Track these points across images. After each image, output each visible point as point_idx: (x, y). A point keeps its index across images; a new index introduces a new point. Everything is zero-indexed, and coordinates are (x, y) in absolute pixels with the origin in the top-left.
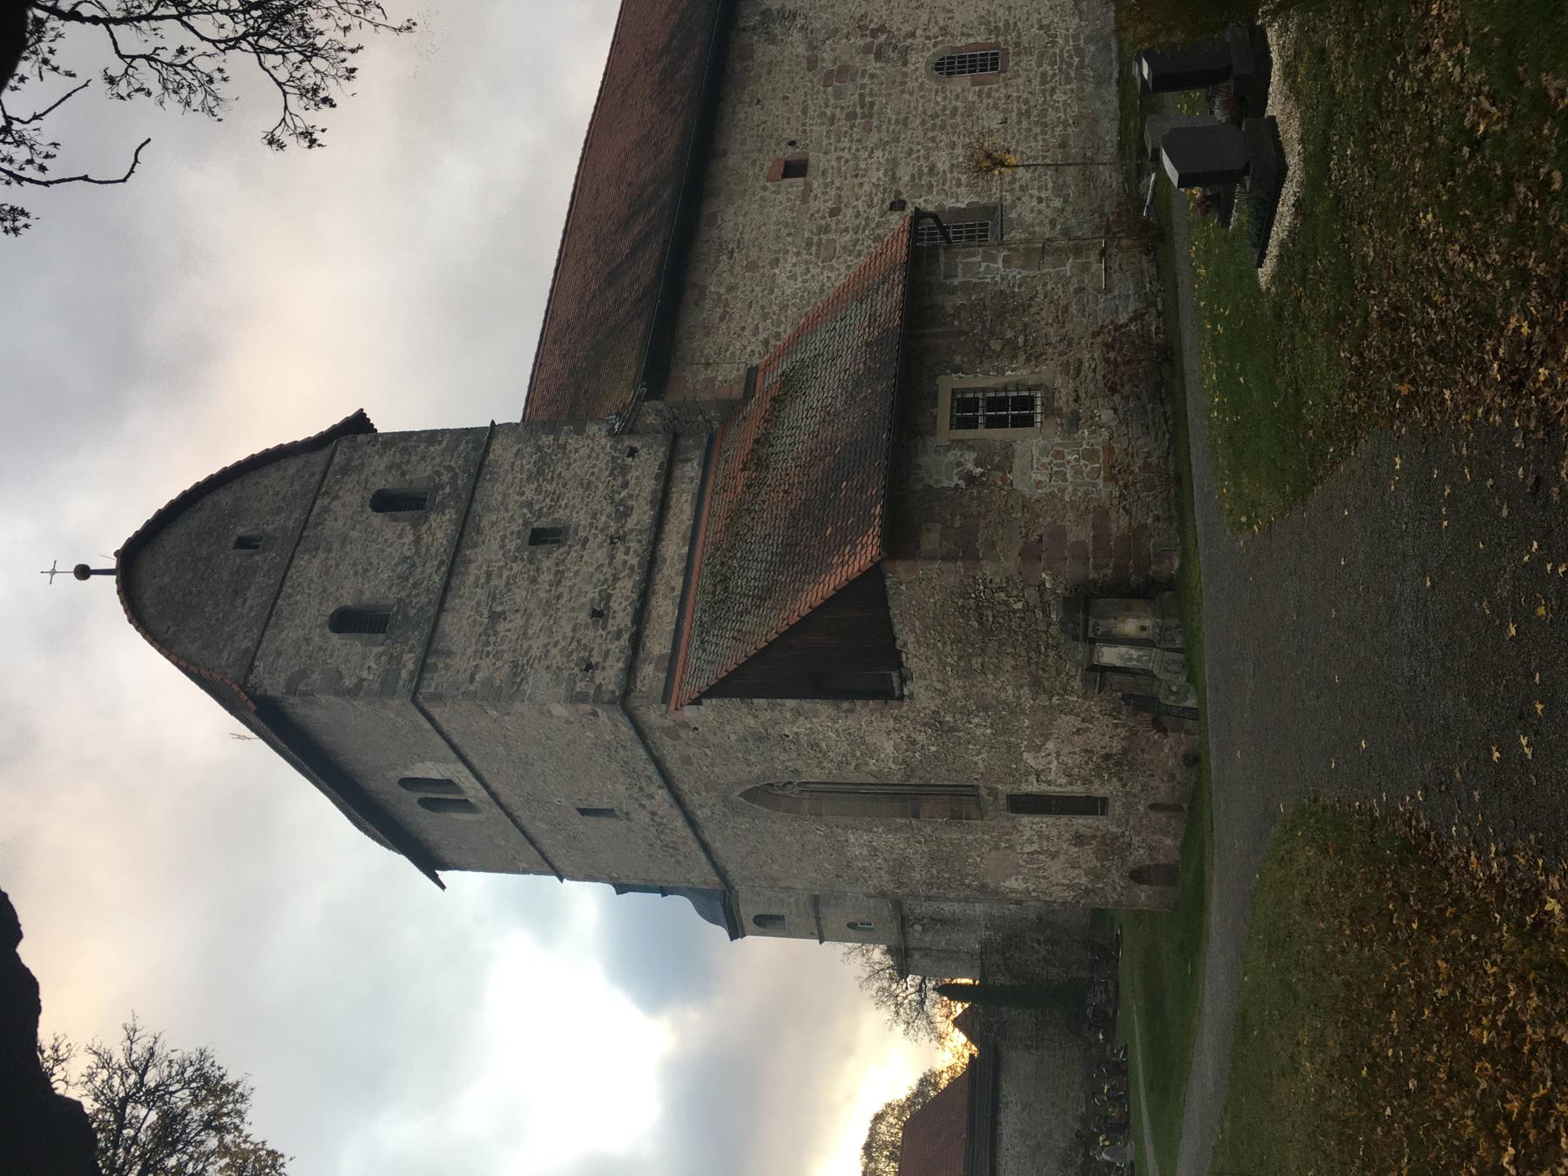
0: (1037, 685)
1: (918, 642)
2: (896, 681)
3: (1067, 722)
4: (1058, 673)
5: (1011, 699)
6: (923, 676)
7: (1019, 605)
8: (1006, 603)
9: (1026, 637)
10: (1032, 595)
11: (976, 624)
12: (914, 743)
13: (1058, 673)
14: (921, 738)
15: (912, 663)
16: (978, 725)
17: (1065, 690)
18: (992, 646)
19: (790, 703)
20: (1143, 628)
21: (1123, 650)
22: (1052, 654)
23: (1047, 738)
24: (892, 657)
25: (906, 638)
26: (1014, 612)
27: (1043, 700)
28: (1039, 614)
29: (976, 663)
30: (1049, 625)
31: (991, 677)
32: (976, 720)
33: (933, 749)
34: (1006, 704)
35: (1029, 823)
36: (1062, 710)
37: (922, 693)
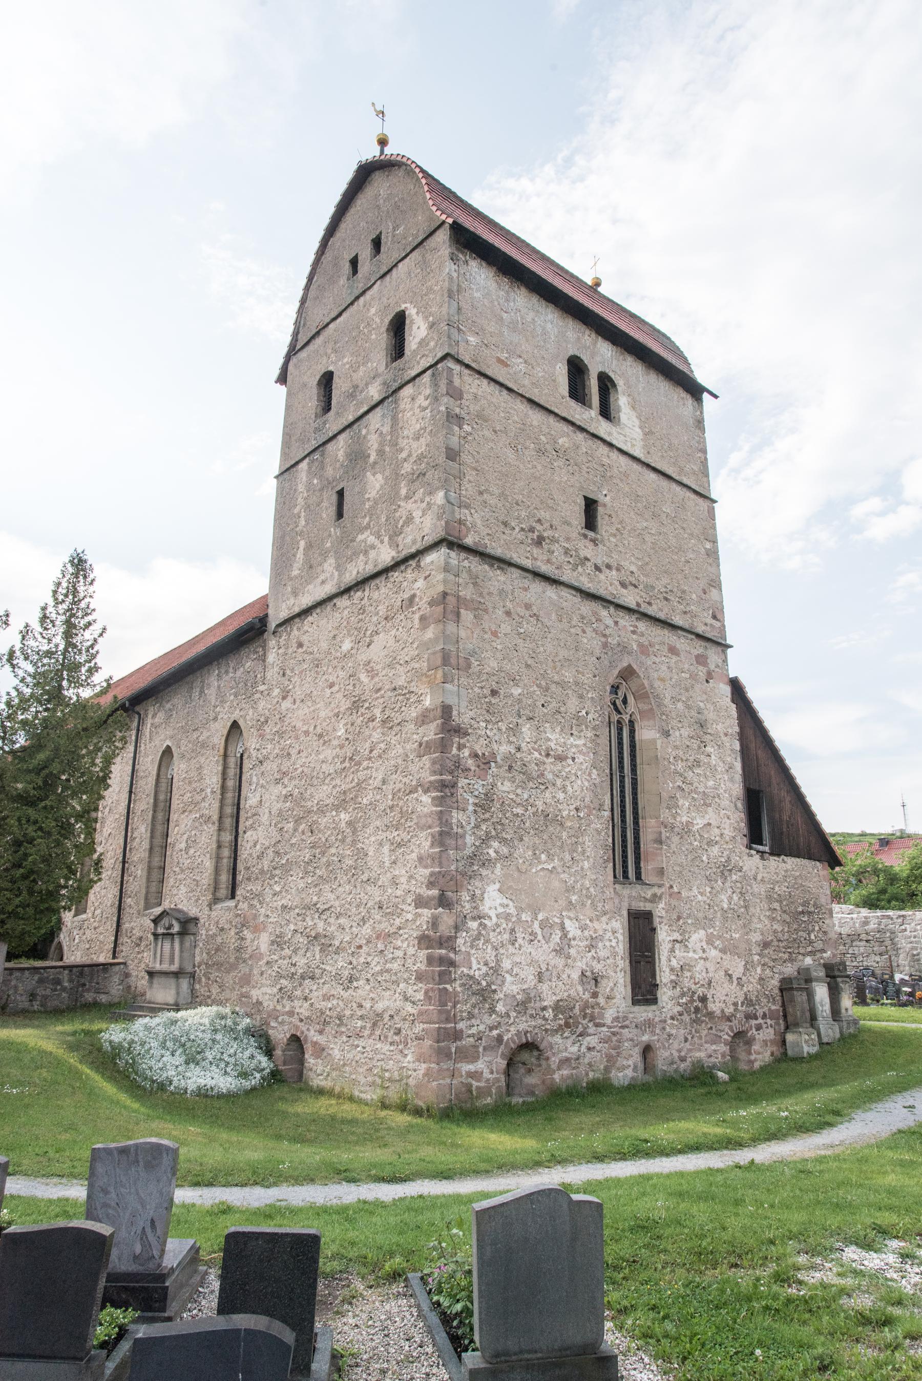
0: (766, 945)
1: (786, 871)
2: (761, 848)
3: (738, 969)
4: (774, 960)
5: (753, 926)
6: (765, 867)
7: (813, 937)
8: (813, 930)
9: (795, 940)
10: (819, 945)
11: (800, 909)
12: (710, 843)
13: (774, 960)
14: (715, 850)
15: (773, 862)
16: (730, 898)
17: (764, 965)
18: (786, 917)
19: (738, 766)
20: (846, 1009)
21: (827, 1000)
22: (786, 956)
23: (723, 951)
24: (778, 851)
25: (791, 863)
26: (809, 934)
27: (756, 949)
28: (809, 949)
29: (776, 905)
30: (803, 955)
31: (768, 913)
32: (735, 897)
33: (705, 858)
34: (750, 922)
35: (615, 936)
36: (748, 966)
37: (752, 863)
